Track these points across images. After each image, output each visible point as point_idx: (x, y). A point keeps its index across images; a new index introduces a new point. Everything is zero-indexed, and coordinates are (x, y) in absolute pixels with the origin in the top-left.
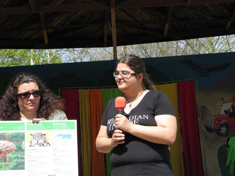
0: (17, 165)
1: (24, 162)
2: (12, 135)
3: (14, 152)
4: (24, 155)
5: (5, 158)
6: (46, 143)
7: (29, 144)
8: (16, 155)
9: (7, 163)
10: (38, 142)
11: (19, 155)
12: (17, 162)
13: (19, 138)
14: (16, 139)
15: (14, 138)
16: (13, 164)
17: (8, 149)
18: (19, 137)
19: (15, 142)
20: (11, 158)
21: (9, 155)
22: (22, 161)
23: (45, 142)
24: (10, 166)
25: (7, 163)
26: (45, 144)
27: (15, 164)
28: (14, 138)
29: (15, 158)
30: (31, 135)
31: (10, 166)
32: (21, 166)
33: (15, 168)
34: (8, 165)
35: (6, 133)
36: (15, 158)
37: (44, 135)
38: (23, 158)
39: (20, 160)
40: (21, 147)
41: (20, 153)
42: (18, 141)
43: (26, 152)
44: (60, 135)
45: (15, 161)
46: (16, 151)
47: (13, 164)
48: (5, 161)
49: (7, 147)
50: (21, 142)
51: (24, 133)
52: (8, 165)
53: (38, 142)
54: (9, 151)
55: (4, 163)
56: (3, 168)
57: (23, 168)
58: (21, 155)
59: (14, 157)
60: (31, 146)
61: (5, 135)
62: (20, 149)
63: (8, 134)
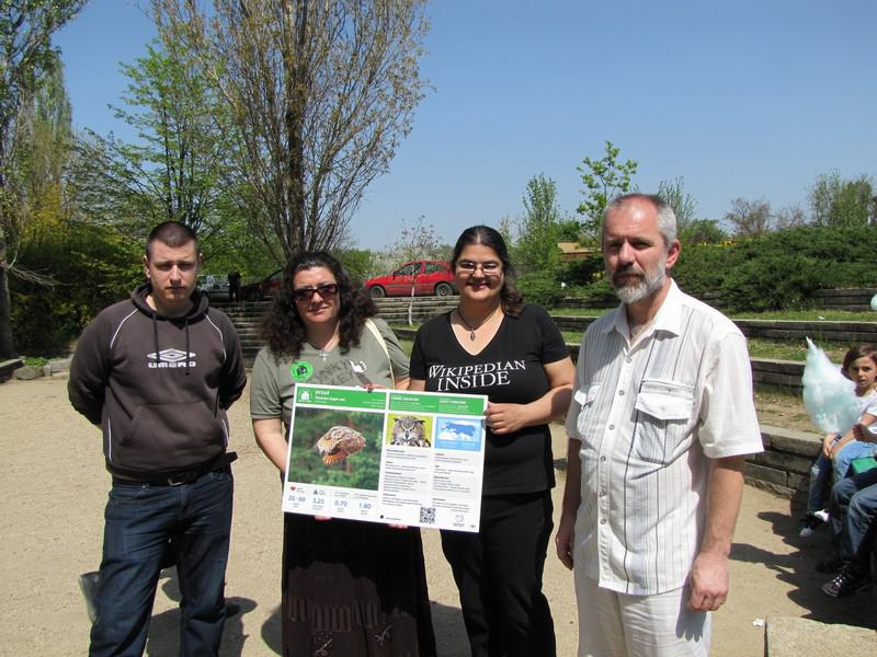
0: (365, 479)
1: (378, 475)
2: (361, 416)
3: (361, 451)
4: (379, 460)
5: (344, 463)
6: (421, 440)
7: (391, 439)
8: (364, 458)
9: (348, 473)
10: (407, 436)
11: (370, 460)
12: (364, 473)
13: (372, 424)
14: (368, 426)
15: (363, 424)
16: (357, 476)
17: (351, 444)
18: (373, 423)
19: (365, 432)
20: (354, 464)
21: (352, 458)
22: (374, 471)
23: (421, 437)
24: (352, 480)
25: (348, 473)
26: (421, 442)
27: (362, 477)
28: (363, 424)
29: (362, 465)
30: (396, 420)
31: (352, 480)
32: (373, 483)
33: (361, 484)
34: (347, 478)
35: (350, 412)
36: (362, 465)
37: (421, 422)
38: (378, 467)
39: (369, 470)
40: (375, 443)
41: (372, 454)
42: (370, 430)
43: (384, 453)
44: (451, 426)
45: (362, 470)
46: (364, 449)
47: (357, 476)
48: (344, 469)
49: (349, 441)
50: (377, 433)
51: (383, 414)
52: (347, 478)
53: (407, 436)
54: (353, 450)
55: (340, 473)
56: (340, 482)
57: (375, 488)
58: (374, 459)
59: (361, 462)
60: (393, 443)
61: (349, 416)
62: (373, 448)
63: (353, 414)
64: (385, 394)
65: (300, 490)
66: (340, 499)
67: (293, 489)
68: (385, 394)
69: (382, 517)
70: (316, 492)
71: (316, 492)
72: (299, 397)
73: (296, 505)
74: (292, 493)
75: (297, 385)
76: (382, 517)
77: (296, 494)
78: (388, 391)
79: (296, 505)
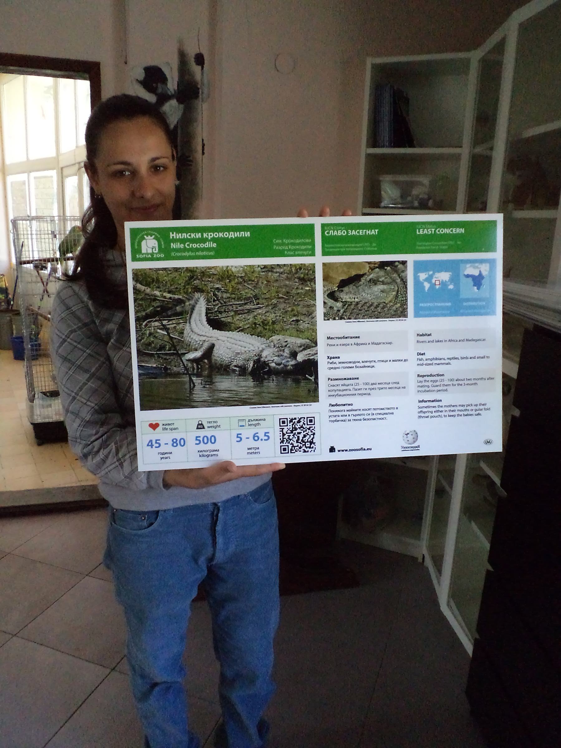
64: (312, 227)
65: (169, 427)
66: (248, 432)
67: (154, 426)
68: (312, 227)
69: (332, 450)
70: (200, 426)
71: (200, 426)
72: (136, 251)
73: (164, 456)
74: (154, 435)
75: (129, 226)
76: (332, 450)
77: (166, 437)
78: (317, 222)
79: (164, 456)
